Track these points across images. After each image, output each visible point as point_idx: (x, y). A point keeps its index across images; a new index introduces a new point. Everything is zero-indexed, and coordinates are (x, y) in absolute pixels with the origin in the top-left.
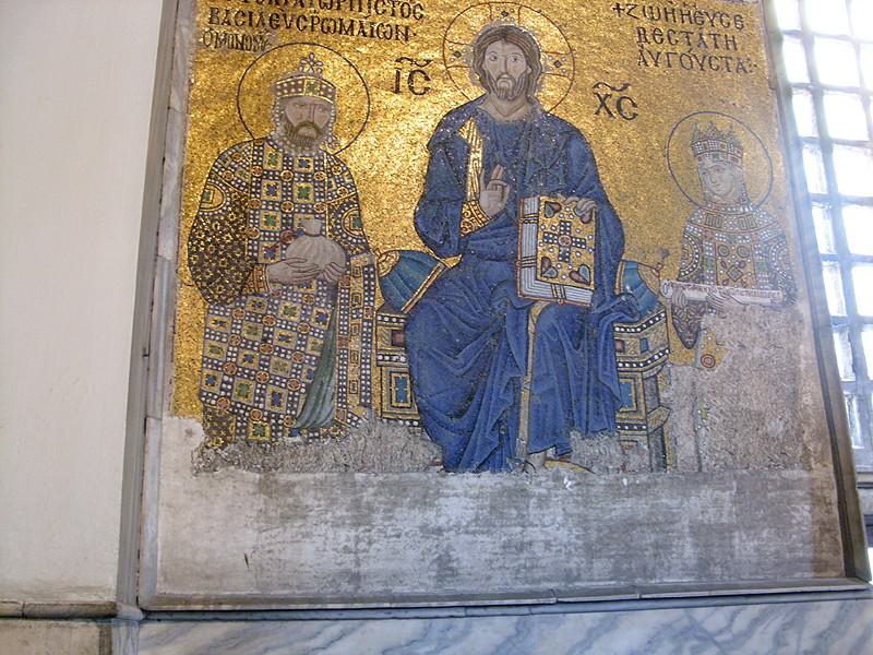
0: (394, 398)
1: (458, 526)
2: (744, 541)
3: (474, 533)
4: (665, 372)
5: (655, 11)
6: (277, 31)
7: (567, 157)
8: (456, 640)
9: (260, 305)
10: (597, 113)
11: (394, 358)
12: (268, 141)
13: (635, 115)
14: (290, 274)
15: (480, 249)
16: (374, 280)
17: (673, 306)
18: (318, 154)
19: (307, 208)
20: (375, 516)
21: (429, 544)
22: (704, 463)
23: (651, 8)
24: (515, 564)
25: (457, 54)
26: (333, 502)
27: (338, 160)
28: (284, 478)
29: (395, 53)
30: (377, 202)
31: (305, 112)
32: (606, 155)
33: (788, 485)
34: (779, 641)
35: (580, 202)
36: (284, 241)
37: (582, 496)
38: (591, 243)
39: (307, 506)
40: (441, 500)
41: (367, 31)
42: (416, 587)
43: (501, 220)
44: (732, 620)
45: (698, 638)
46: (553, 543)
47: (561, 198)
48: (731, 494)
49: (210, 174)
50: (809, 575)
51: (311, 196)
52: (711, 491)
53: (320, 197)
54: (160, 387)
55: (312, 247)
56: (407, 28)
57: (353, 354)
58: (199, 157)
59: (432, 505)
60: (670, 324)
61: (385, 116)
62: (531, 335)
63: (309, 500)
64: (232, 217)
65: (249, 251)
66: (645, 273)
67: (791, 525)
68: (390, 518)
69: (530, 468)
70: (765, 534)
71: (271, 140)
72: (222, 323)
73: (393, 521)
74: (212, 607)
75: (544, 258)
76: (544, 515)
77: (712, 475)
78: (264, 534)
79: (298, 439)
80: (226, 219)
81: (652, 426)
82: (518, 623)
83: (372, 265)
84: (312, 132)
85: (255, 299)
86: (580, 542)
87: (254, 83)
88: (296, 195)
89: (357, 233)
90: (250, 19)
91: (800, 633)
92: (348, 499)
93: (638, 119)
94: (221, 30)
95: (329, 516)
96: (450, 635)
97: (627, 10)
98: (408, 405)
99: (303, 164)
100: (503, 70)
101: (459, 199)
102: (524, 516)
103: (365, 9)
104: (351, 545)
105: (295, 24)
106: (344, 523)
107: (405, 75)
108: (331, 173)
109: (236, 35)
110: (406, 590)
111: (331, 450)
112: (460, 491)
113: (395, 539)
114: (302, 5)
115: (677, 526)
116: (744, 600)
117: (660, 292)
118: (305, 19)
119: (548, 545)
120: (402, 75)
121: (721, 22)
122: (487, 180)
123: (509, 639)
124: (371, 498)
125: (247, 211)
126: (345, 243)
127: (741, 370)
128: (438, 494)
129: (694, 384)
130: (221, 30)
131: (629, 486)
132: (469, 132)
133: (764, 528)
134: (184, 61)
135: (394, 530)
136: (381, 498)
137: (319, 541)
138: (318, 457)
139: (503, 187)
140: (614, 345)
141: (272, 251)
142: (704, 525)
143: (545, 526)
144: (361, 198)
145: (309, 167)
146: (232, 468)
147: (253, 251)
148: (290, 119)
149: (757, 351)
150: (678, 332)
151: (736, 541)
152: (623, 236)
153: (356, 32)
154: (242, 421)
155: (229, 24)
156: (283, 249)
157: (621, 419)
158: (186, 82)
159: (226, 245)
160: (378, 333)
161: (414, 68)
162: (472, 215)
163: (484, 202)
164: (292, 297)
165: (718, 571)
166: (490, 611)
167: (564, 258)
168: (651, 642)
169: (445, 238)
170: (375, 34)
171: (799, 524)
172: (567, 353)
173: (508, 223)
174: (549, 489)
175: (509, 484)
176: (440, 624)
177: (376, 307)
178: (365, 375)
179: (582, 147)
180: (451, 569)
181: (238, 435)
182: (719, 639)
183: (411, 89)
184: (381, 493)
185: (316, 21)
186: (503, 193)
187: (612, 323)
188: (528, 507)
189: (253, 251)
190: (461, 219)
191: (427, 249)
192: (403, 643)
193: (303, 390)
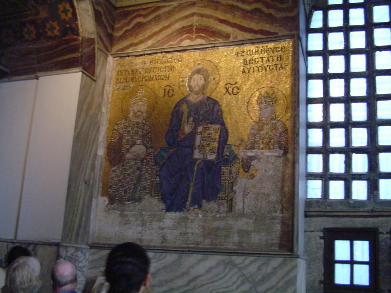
1: (168, 227)
4: (236, 181)
9: (123, 166)
10: (225, 94)
17: (242, 158)
21: (161, 232)
22: (245, 210)
24: (183, 239)
26: (137, 220)
28: (126, 213)
31: (139, 107)
33: (274, 218)
34: (259, 269)
36: (131, 147)
38: (217, 140)
40: (164, 220)
44: (244, 260)
45: (232, 265)
46: (194, 233)
47: (210, 125)
50: (277, 249)
54: (97, 189)
56: (169, 75)
57: (146, 179)
59: (162, 221)
60: (240, 165)
62: (195, 171)
63: (131, 219)
66: (234, 148)
68: (151, 224)
69: (190, 211)
70: (263, 234)
72: (114, 171)
74: (103, 246)
75: (202, 146)
76: (192, 225)
78: (121, 228)
79: (130, 202)
81: (229, 198)
82: (179, 256)
86: (202, 234)
89: (150, 143)
95: (136, 223)
96: (161, 257)
100: (196, 84)
102: (186, 225)
103: (157, 71)
104: (140, 231)
107: (167, 91)
111: (138, 206)
115: (233, 230)
116: (248, 255)
118: (141, 77)
119: (193, 234)
122: (187, 122)
128: (164, 218)
129: (245, 184)
131: (219, 217)
134: (108, 98)
136: (149, 219)
138: (135, 207)
139: (192, 124)
140: (221, 172)
141: (128, 151)
143: (193, 228)
146: (114, 210)
149: (271, 172)
151: (252, 236)
156: (131, 149)
157: (220, 196)
158: (109, 103)
165: (244, 245)
166: (171, 252)
167: (208, 145)
168: (218, 265)
171: (276, 231)
172: (205, 176)
173: (192, 135)
174: (194, 217)
175: (183, 215)
176: (159, 254)
180: (166, 239)
182: (239, 266)
183: (168, 96)
184: (149, 217)
186: (192, 127)
187: (221, 165)
193: (132, 189)
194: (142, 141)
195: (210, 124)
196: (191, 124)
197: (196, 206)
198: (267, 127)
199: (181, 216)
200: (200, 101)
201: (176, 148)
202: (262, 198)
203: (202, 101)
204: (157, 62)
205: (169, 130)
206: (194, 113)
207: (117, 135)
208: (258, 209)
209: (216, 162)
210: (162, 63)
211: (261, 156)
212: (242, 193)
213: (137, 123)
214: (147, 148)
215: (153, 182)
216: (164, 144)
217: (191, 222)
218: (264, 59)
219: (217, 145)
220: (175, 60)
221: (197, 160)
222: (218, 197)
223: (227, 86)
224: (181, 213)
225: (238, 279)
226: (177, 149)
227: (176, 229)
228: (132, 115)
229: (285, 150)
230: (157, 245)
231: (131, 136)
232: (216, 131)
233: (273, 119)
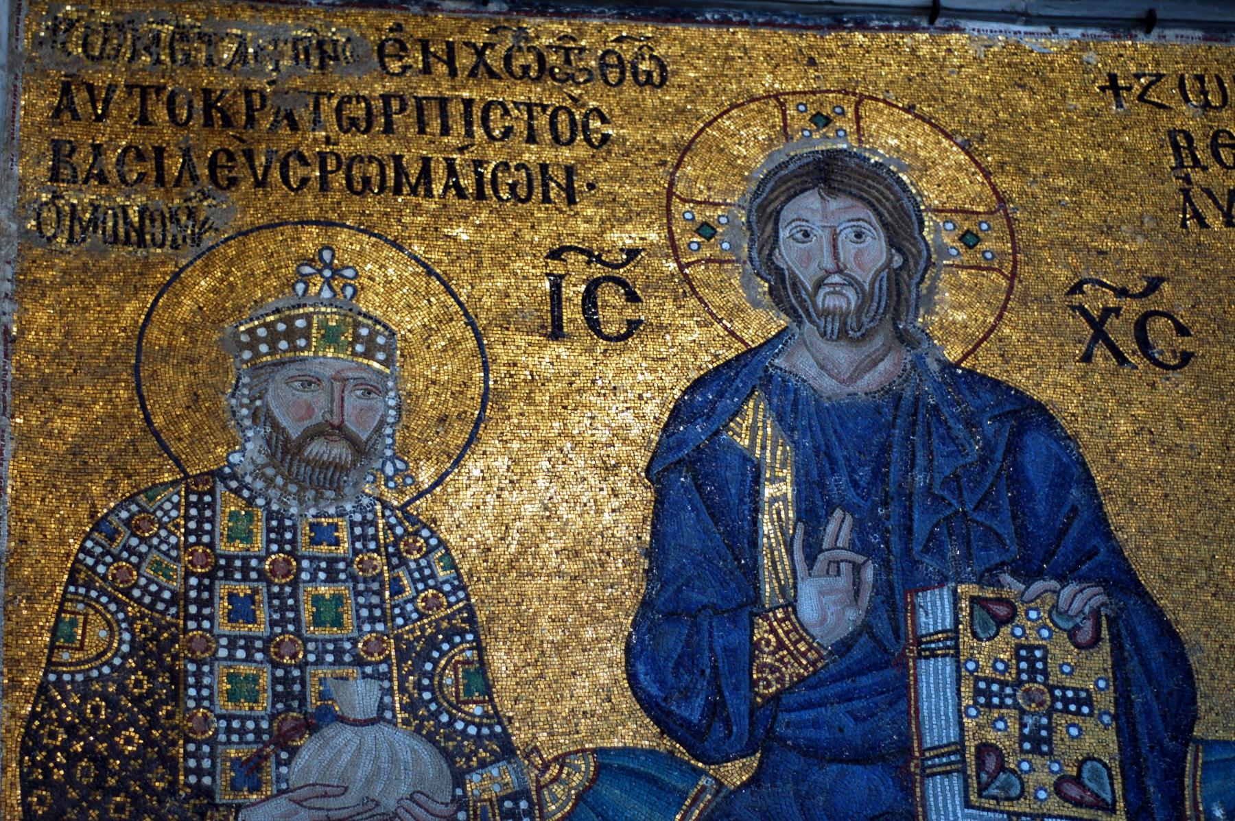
5: (1211, 85)
6: (233, 195)
7: (1017, 478)
10: (1087, 357)
12: (224, 479)
13: (1186, 358)
15: (811, 733)
18: (359, 507)
19: (339, 652)
23: (1200, 79)
25: (706, 230)
27: (414, 520)
29: (544, 235)
30: (524, 625)
32: (1120, 466)
35: (1067, 592)
38: (1106, 701)
41: (468, 182)
43: (857, 653)
47: (1012, 586)
49: (73, 572)
51: (348, 619)
53: (372, 620)
55: (359, 748)
56: (570, 171)
58: (41, 529)
61: (529, 399)
64: (138, 683)
65: (188, 772)
71: (233, 476)
75: (984, 749)
80: (122, 689)
83: (524, 793)
84: (339, 451)
87: (179, 331)
88: (306, 616)
89: (477, 710)
90: (160, 167)
93: (1195, 367)
94: (82, 197)
97: (1137, 89)
99: (320, 534)
101: (741, 606)
103: (458, 127)
105: (276, 174)
107: (573, 291)
108: (398, 554)
109: (124, 209)
114: (294, 126)
120: (567, 291)
122: (812, 552)
125: (179, 665)
126: (448, 738)
130: (82, 197)
132: (753, 429)
139: (857, 569)
144: (481, 617)
145: (337, 542)
147: (199, 772)
148: (284, 424)
152: (1189, 675)
153: (438, 189)
155: (103, 179)
156: (279, 763)
159: (126, 759)
161: (597, 271)
162: (781, 645)
163: (808, 609)
167: (1038, 743)
169: (715, 709)
170: (488, 191)
179: (1054, 447)
183: (594, 325)
185: (331, 164)
186: (857, 593)
189: (199, 772)
190: (753, 658)
191: (667, 743)
195: (1014, 574)
201: (754, 761)
203: (908, 394)
204: (450, 62)
206: (855, 484)
210: (492, 74)
219: (1111, 737)
220: (603, 65)
223: (1094, 301)
226: (761, 762)
228: (261, 460)
231: (268, 640)
232: (1077, 627)
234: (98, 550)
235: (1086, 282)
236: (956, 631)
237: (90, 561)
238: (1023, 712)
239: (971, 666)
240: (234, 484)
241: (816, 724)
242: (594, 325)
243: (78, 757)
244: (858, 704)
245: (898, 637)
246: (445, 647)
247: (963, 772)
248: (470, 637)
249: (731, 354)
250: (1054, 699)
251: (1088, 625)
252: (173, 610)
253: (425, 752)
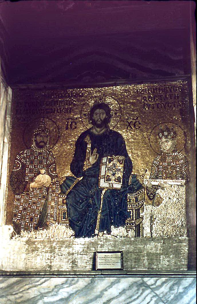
0: (62, 218)
1: (78, 253)
2: (164, 258)
3: (82, 255)
8: (74, 284)
11: (63, 207)
14: (36, 185)
16: (58, 185)
20: (56, 250)
21: (70, 257)
22: (153, 235)
25: (85, 115)
26: (45, 246)
37: (113, 244)
39: (38, 248)
40: (74, 246)
42: (65, 269)
43: (95, 165)
44: (156, 282)
45: (145, 286)
48: (161, 244)
52: (154, 243)
53: (45, 163)
59: (71, 247)
63: (39, 246)
67: (181, 254)
68: (60, 251)
70: (171, 257)
73: (61, 251)
75: (108, 176)
77: (155, 238)
78: (27, 255)
82: (92, 279)
85: (27, 192)
89: (54, 172)
91: (178, 287)
92: (49, 245)
95: (44, 250)
96: (73, 282)
98: (66, 220)
106: (48, 252)
110: (63, 270)
112: (79, 243)
113: (61, 256)
117: (143, 183)
121: (174, 89)
122: (92, 153)
123: (89, 284)
124: (55, 245)
127: (168, 206)
128: (73, 244)
130: (19, 116)
133: (171, 255)
135: (61, 254)
136: (58, 245)
137: (41, 257)
139: (97, 155)
141: (32, 180)
142: (151, 253)
144: (56, 162)
145: (42, 154)
147: (27, 180)
150: (148, 195)
151: (162, 258)
154: (23, 226)
159: (20, 178)
160: (59, 200)
161: (73, 121)
162: (87, 164)
163: (90, 160)
164: (37, 192)
167: (114, 175)
168: (130, 287)
173: (97, 166)
174: (104, 243)
177: (59, 193)
178: (55, 212)
181: (22, 229)
183: (71, 127)
186: (96, 157)
188: (98, 247)
192: (60, 284)
194: (45, 171)
196: (95, 155)
197: (105, 232)
198: (169, 159)
199: (90, 242)
200: (103, 133)
201: (82, 178)
202: (168, 223)
205: (73, 160)
207: (19, 164)
208: (165, 232)
209: (122, 190)
211: (165, 185)
212: (149, 218)
213: (40, 153)
214: (52, 177)
215: (60, 209)
216: (69, 174)
217: (101, 247)
218: (162, 96)
221: (103, 189)
222: (126, 223)
224: (90, 238)
225: (151, 300)
227: (86, 254)
229: (187, 180)
230: (68, 270)
232: (120, 161)
233: (174, 151)
234: (18, 156)
235: (129, 118)
236: (107, 162)
237: (17, 158)
238: (113, 171)
239: (108, 166)
240: (32, 148)
241: (90, 173)
242: (71, 127)
243: (15, 178)
244: (94, 171)
245: (100, 163)
246: (52, 166)
247: (105, 179)
248: (54, 164)
249: (86, 130)
250: (116, 170)
251: (122, 161)
252: (25, 163)
253: (49, 176)
